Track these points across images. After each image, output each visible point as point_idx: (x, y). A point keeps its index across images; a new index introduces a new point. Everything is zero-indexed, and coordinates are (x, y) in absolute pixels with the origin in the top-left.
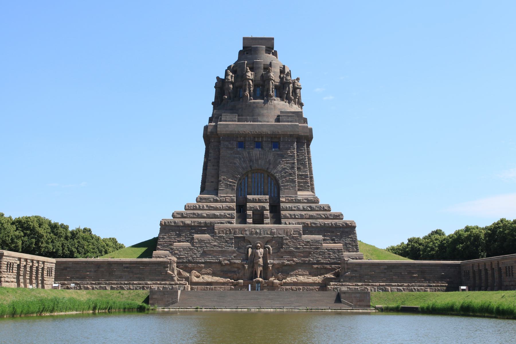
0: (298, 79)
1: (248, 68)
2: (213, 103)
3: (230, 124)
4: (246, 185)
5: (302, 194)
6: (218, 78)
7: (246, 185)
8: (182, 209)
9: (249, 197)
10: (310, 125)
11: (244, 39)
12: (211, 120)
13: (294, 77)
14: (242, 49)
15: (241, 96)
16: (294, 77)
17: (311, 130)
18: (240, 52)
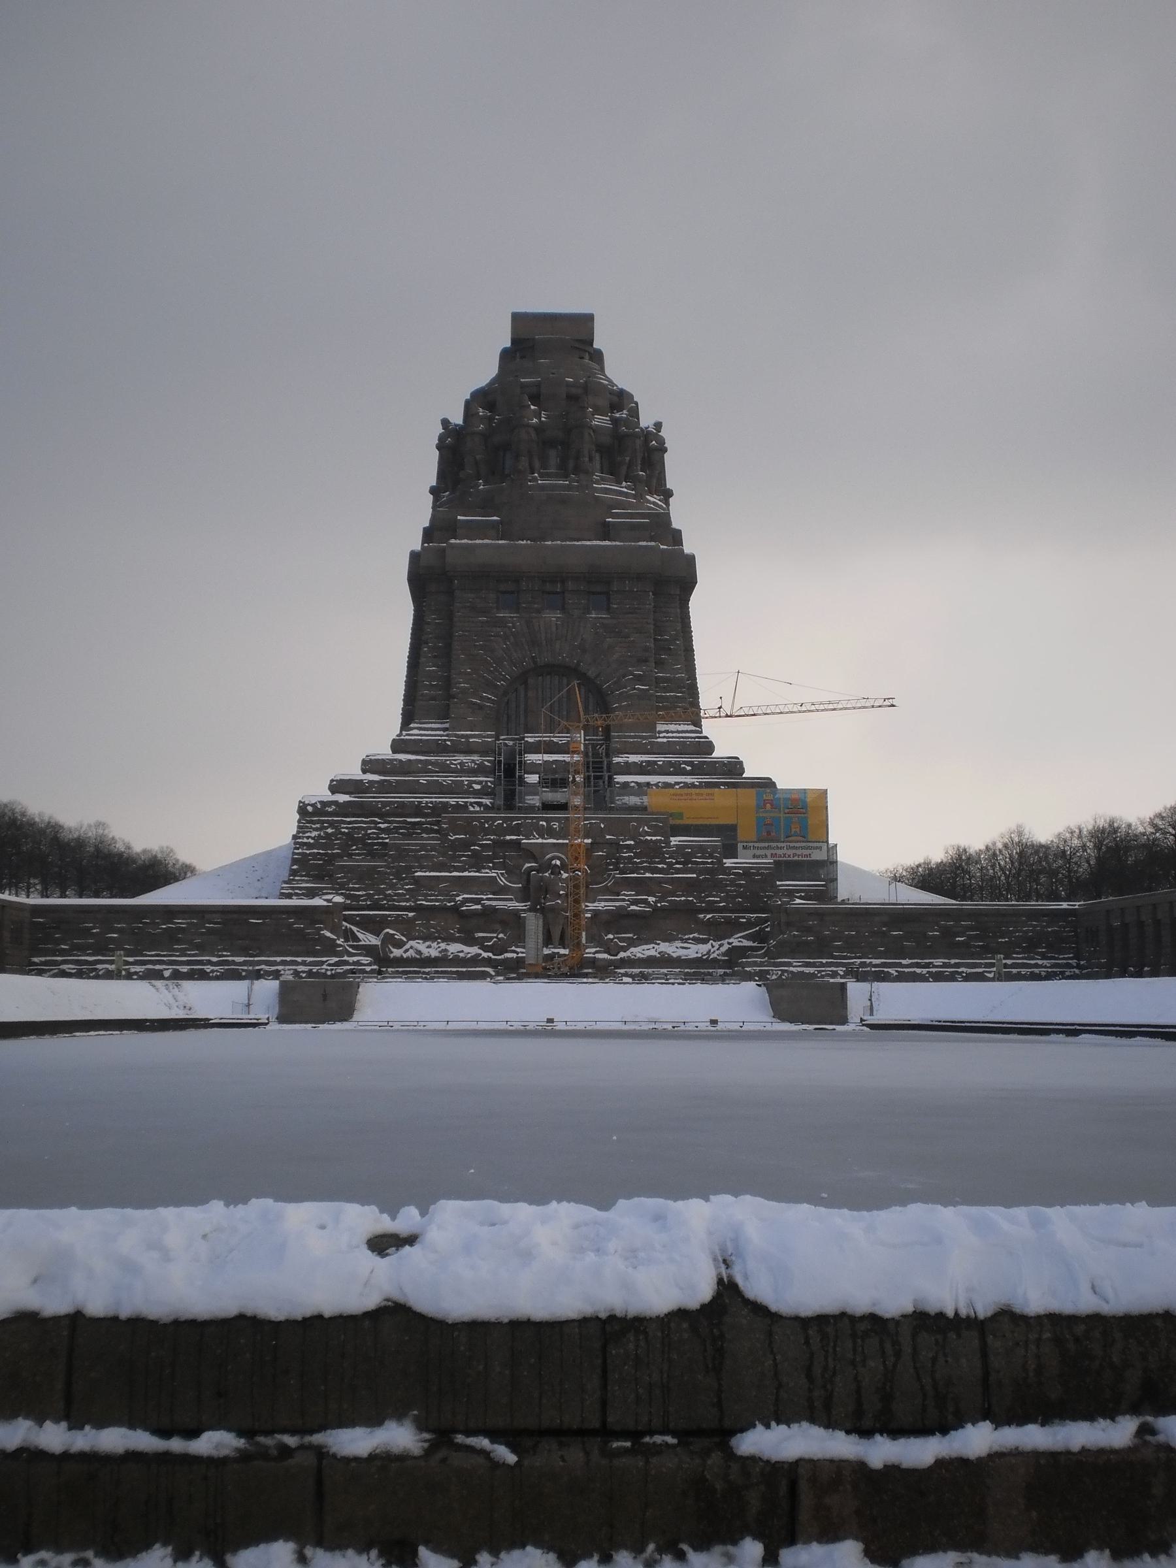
0: (658, 426)
1: (526, 397)
2: (433, 491)
3: (480, 547)
4: (522, 707)
5: (670, 730)
6: (445, 423)
7: (522, 707)
8: (354, 771)
9: (530, 739)
10: (687, 549)
11: (517, 318)
12: (428, 534)
13: (646, 421)
14: (508, 344)
15: (507, 472)
16: (646, 421)
17: (691, 560)
18: (506, 355)
